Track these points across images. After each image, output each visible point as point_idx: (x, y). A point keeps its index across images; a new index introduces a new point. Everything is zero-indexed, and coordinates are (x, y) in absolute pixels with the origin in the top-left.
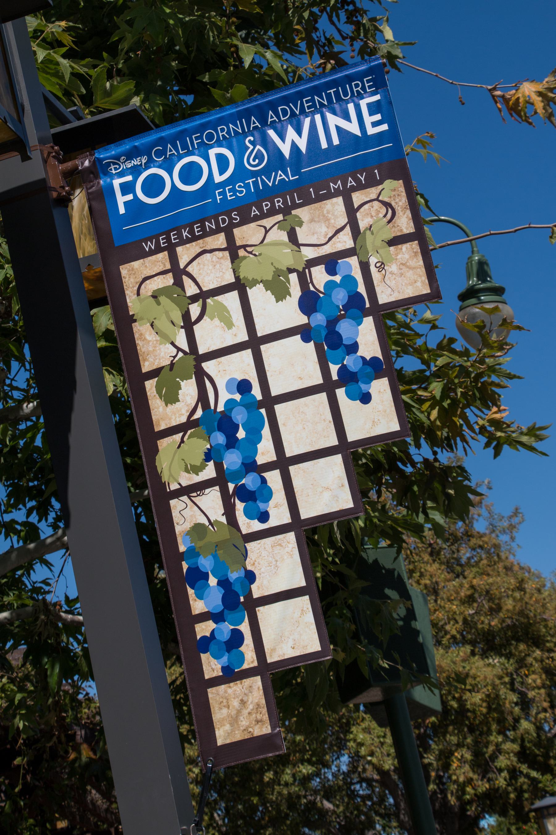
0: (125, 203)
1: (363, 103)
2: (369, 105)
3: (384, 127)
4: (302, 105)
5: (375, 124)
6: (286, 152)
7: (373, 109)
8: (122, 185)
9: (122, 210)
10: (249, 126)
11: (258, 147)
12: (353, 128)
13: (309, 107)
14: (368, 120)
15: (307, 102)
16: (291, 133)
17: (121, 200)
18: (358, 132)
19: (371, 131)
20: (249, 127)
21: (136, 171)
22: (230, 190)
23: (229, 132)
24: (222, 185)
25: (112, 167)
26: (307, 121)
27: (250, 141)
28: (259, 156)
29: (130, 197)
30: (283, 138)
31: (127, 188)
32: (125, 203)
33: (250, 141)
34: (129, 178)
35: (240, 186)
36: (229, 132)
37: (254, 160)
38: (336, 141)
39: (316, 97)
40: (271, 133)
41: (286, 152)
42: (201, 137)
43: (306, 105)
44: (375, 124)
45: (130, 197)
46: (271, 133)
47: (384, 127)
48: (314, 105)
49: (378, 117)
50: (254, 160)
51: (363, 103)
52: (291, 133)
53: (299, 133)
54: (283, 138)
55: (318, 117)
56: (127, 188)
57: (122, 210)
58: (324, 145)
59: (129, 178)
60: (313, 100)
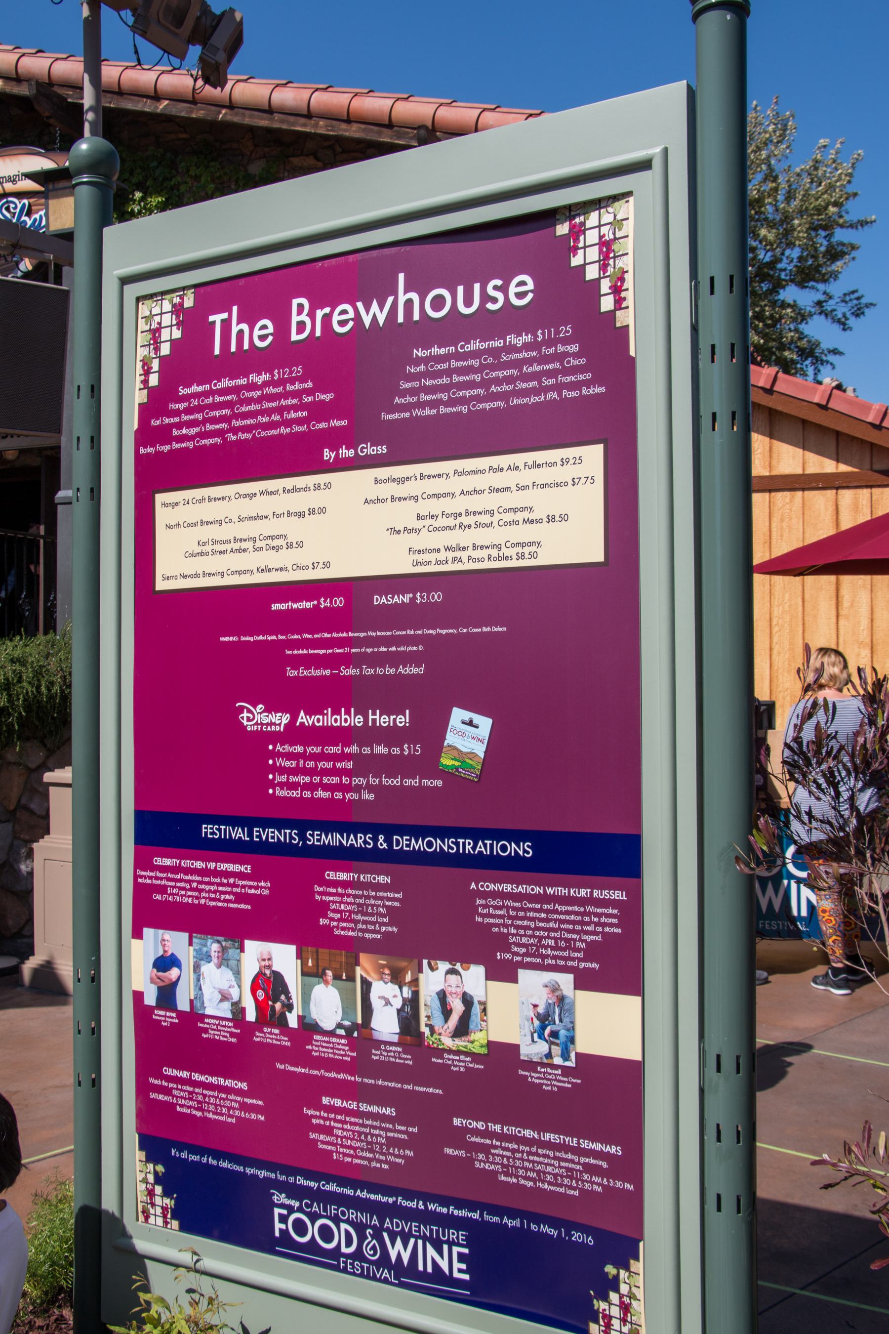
0: (280, 1230)
1: (455, 1249)
2: (460, 1255)
3: (466, 1277)
4: (411, 1225)
5: (460, 1271)
6: (393, 1258)
7: (461, 1257)
8: (280, 1215)
9: (277, 1234)
10: (371, 1222)
11: (374, 1241)
12: (444, 1265)
13: (415, 1231)
14: (457, 1265)
15: (415, 1226)
16: (399, 1241)
17: (278, 1226)
18: (447, 1271)
19: (456, 1274)
20: (371, 1222)
21: (291, 1209)
22: (351, 1264)
23: (356, 1217)
24: (347, 1256)
25: (276, 1197)
26: (412, 1241)
27: (369, 1233)
28: (374, 1248)
29: (283, 1226)
30: (393, 1245)
31: (283, 1219)
32: (280, 1230)
33: (369, 1233)
34: (285, 1212)
35: (357, 1265)
36: (356, 1217)
37: (370, 1250)
38: (430, 1269)
39: (422, 1227)
40: (385, 1235)
41: (393, 1258)
42: (337, 1210)
43: (413, 1228)
44: (460, 1271)
45: (283, 1226)
46: (385, 1235)
47: (466, 1277)
48: (419, 1231)
49: (463, 1266)
50: (370, 1250)
51: (455, 1249)
52: (399, 1241)
53: (405, 1248)
54: (393, 1244)
55: (420, 1242)
56: (283, 1219)
57: (277, 1234)
58: (421, 1268)
59: (285, 1212)
60: (419, 1227)
